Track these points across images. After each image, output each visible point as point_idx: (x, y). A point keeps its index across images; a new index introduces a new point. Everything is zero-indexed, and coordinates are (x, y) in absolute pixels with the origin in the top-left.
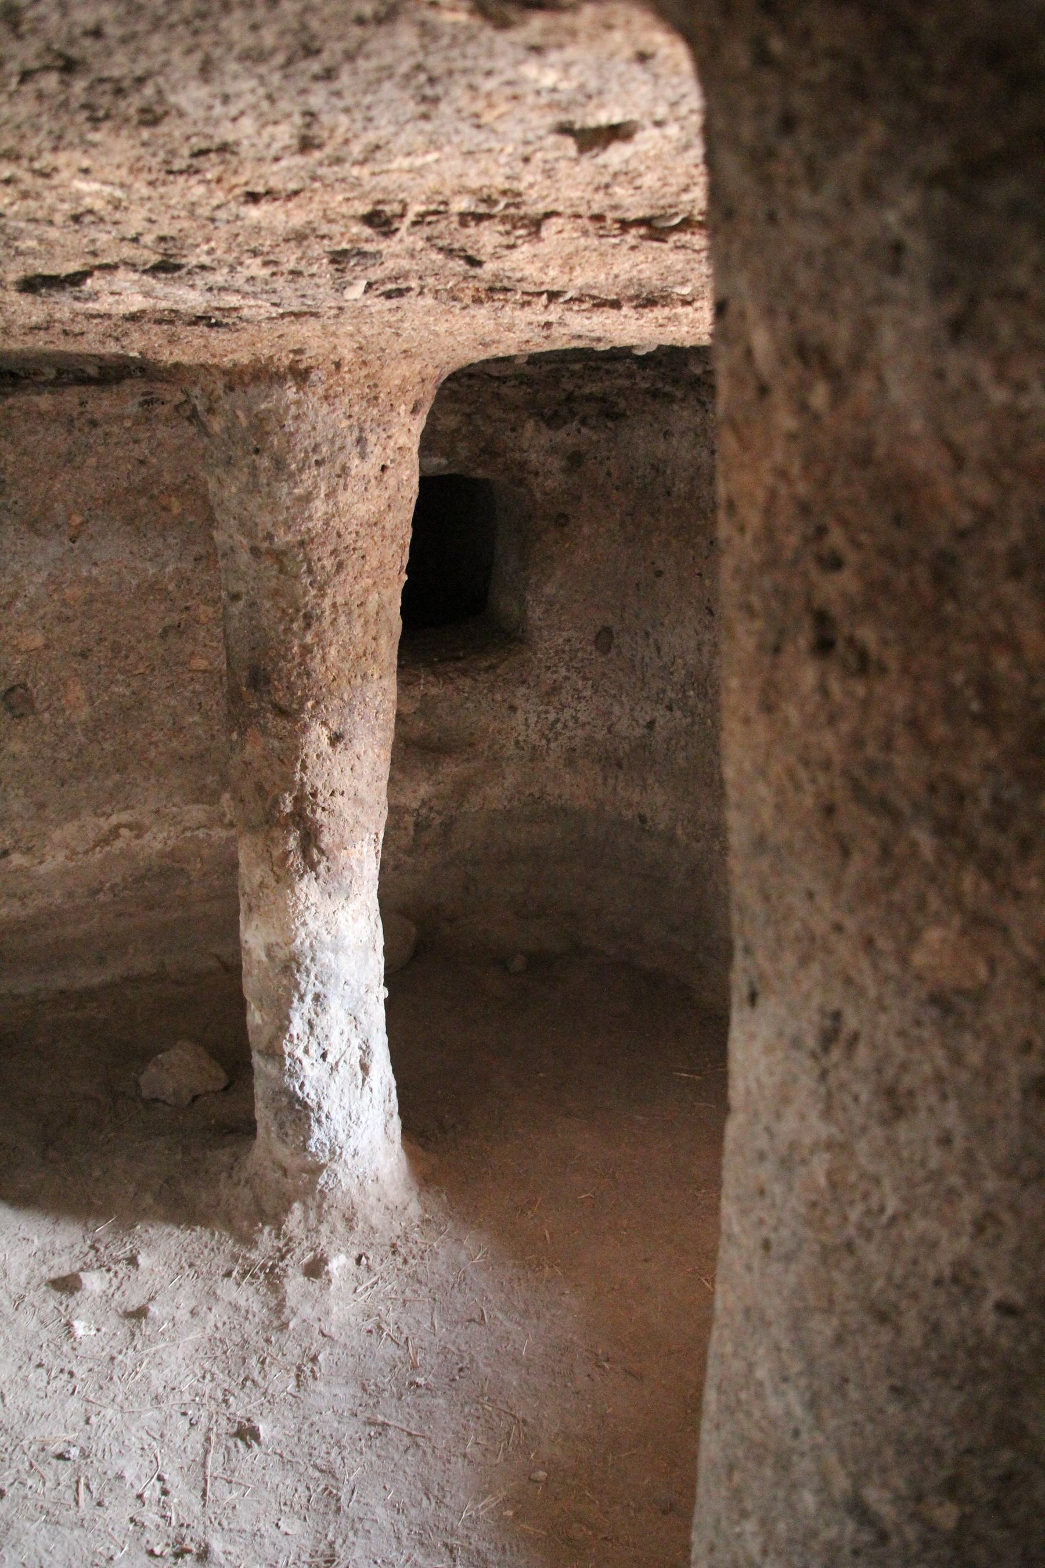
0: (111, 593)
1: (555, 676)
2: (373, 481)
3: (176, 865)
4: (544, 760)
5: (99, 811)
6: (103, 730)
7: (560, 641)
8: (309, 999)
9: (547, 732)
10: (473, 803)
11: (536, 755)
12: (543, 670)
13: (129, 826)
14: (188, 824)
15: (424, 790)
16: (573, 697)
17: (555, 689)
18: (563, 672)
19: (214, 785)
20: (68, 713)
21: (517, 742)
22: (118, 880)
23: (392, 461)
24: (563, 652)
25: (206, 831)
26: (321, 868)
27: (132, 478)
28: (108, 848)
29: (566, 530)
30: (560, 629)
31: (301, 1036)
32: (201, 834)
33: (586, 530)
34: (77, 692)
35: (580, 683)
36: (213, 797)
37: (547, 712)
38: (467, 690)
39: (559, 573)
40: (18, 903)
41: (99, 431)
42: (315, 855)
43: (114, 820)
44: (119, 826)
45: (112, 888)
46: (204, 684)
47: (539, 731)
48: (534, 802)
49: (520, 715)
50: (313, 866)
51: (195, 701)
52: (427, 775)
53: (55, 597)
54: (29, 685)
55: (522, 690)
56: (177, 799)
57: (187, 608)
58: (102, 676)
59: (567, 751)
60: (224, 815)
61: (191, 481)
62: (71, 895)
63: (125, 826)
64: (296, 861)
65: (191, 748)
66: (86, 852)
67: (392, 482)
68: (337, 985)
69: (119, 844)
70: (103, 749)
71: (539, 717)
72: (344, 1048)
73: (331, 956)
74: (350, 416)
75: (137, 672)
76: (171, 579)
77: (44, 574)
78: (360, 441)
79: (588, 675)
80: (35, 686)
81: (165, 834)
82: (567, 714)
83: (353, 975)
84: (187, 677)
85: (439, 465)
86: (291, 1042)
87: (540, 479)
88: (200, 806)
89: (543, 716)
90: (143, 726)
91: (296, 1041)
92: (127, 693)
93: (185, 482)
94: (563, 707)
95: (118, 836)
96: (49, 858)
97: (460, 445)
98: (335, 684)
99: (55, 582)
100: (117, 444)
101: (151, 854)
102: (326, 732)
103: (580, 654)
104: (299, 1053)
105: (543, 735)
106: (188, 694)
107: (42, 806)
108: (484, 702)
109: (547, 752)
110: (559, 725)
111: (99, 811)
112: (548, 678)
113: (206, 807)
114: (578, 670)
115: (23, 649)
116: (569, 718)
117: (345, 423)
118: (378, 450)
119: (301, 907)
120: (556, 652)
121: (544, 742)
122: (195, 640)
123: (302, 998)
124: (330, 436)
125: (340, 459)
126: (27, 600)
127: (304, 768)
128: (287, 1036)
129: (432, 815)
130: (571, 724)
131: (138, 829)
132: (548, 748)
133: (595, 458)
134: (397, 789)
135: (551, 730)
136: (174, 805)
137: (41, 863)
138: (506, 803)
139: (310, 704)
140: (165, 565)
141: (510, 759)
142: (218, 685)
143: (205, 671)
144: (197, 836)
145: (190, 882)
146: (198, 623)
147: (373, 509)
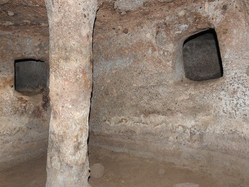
0: (119, 71)
1: (234, 87)
2: (57, 12)
4: (235, 118)
7: (233, 74)
9: (234, 108)
10: (210, 129)
11: (231, 116)
12: (229, 85)
14: (135, 121)
15: (193, 123)
16: (242, 94)
17: (235, 92)
18: (236, 85)
19: (139, 113)
21: (224, 111)
23: (61, 5)
24: (235, 78)
28: (121, 123)
29: (228, 34)
30: (232, 70)
33: (235, 32)
34: (115, 91)
35: (244, 89)
36: (139, 116)
37: (233, 100)
38: (203, 92)
39: (228, 50)
41: (112, 39)
43: (122, 117)
44: (122, 119)
45: (122, 132)
47: (231, 107)
48: (233, 134)
49: (223, 102)
51: (134, 93)
52: (193, 118)
53: (111, 72)
55: (223, 93)
56: (132, 115)
59: (243, 115)
62: (115, 131)
63: (124, 119)
65: (134, 104)
66: (117, 123)
67: (63, 11)
69: (123, 123)
71: (230, 102)
76: (128, 67)
77: (109, 68)
79: (246, 86)
82: (241, 101)
83: (57, 143)
84: (132, 88)
85: (186, 27)
87: (214, 20)
89: (232, 102)
92: (122, 91)
94: (239, 98)
97: (189, 19)
99: (111, 69)
103: (242, 78)
105: (233, 109)
106: (133, 92)
108: (210, 96)
109: (236, 115)
110: (238, 105)
112: (231, 88)
114: (242, 84)
116: (242, 102)
118: (56, 4)
120: (232, 78)
121: (234, 111)
129: (196, 131)
130: (243, 105)
132: (236, 114)
133: (230, 4)
134: (184, 121)
135: (235, 107)
138: (222, 132)
140: (127, 64)
141: (222, 116)
145: (136, 135)
147: (59, 19)
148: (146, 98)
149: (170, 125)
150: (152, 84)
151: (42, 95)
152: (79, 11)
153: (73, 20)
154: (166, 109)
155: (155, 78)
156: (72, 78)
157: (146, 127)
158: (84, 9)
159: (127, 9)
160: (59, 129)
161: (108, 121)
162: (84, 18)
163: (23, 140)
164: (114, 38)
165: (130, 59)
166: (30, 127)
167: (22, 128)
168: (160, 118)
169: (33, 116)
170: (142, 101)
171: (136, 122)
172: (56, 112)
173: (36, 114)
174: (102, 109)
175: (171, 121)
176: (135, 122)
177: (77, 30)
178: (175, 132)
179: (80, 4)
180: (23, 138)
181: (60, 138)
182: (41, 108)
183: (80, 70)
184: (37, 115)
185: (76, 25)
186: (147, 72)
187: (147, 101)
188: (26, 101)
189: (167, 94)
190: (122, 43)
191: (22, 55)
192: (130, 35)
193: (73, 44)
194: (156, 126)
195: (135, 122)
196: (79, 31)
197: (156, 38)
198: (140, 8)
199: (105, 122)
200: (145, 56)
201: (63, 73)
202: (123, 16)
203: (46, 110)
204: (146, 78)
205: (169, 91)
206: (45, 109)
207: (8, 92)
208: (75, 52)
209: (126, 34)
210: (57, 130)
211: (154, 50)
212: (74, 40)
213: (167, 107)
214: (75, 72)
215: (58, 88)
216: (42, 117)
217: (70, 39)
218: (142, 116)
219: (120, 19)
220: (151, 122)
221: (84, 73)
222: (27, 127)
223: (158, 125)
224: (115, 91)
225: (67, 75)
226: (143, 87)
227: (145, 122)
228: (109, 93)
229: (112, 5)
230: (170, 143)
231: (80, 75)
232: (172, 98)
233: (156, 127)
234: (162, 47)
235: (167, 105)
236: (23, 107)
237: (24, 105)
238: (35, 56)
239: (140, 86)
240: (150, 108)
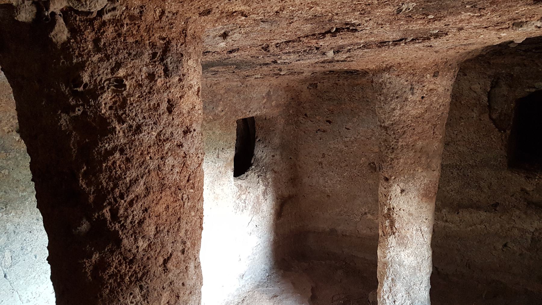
2: (418, 102)
8: (390, 279)
23: (426, 95)
26: (396, 234)
31: (387, 291)
40: (369, 230)
42: (395, 230)
50: (394, 233)
60: (443, 217)
64: (388, 230)
68: (400, 278)
72: (403, 302)
73: (398, 267)
74: (407, 81)
78: (412, 89)
83: (407, 277)
86: (384, 292)
91: (385, 293)
98: (402, 172)
102: (399, 188)
104: (386, 297)
117: (406, 83)
119: (389, 246)
123: (387, 278)
124: (401, 88)
125: (405, 95)
127: (391, 199)
128: (382, 290)
137: (377, 219)
139: (393, 178)
150: (471, 162)
151: (256, 175)
168: (483, 215)
174: (359, 194)
182: (261, 197)
199: (365, 216)
203: (266, 200)
207: (229, 180)
210: (407, 261)
220: (461, 220)
227: (448, 220)
233: (469, 229)
234: (496, 108)
236: (243, 201)
237: (243, 197)
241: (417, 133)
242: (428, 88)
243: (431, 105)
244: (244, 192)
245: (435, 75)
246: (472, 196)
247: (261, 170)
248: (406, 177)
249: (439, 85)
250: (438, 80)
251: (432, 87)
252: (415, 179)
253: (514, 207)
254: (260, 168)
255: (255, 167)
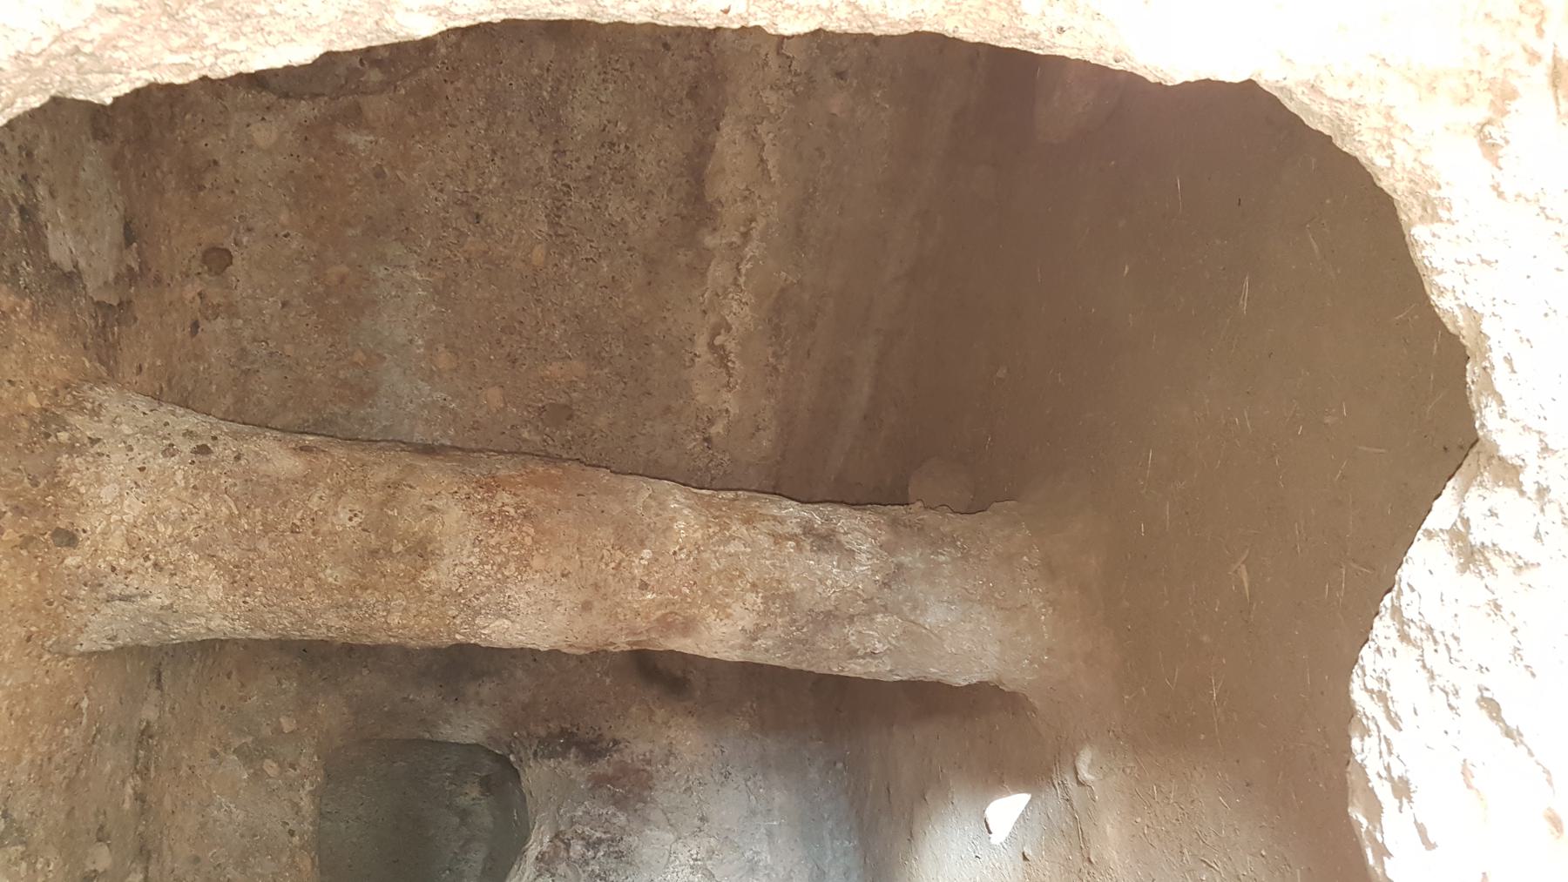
2: (177, 579)
3: (774, 295)
5: (687, 364)
6: (599, 353)
13: (715, 333)
14: (731, 280)
20: (574, 379)
22: (770, 350)
23: (147, 558)
25: (745, 262)
27: (304, 313)
32: (744, 268)
34: (554, 369)
36: (705, 256)
40: (762, 432)
43: (701, 347)
44: (711, 346)
45: (775, 354)
46: (562, 256)
54: (540, 405)
56: (697, 293)
57: (468, 261)
58: (539, 347)
61: (304, 256)
62: (770, 391)
63: (713, 337)
66: (730, 376)
67: (175, 552)
69: (731, 346)
70: (620, 355)
75: (540, 315)
76: (430, 275)
80: (542, 401)
81: (734, 304)
88: (712, 268)
90: (603, 316)
93: (307, 262)
95: (722, 347)
96: (726, 405)
100: (264, 329)
101: (752, 317)
106: (574, 269)
107: (668, 409)
111: (687, 364)
113: (713, 263)
115: (502, 405)
118: (134, 581)
122: (507, 258)
126: (450, 398)
131: (722, 327)
136: (703, 296)
137: (727, 411)
140: (414, 280)
142: (567, 240)
143: (548, 253)
144: (745, 282)
145: (800, 283)
146: (487, 253)
147: (213, 575)
148: (617, 206)
149: (771, 97)
150: (544, 158)
152: (179, 476)
153: (229, 508)
154: (688, 105)
155: (513, 135)
156: (516, 534)
157: (768, 226)
158: (169, 451)
159: (119, 237)
160: (738, 609)
161: (711, 422)
162: (213, 457)
163: (757, 853)
164: (247, 333)
165: (382, 259)
166: (697, 822)
167: (696, 860)
169: (640, 805)
170: (632, 227)
171: (736, 279)
172: (664, 616)
173: (630, 791)
175: (754, 88)
176: (735, 283)
177: (277, 491)
178: (811, 80)
179: (142, 469)
180: (748, 854)
181: (776, 607)
182: (603, 767)
183: (482, 500)
184: (636, 790)
185: (255, 497)
186: (472, 176)
187: (635, 203)
188: (557, 836)
189: (611, 87)
190: (282, 291)
191: (302, 847)
192: (245, 240)
193: (350, 519)
194: (766, 172)
195: (735, 283)
196: (282, 487)
197: (287, 96)
198: (116, 162)
199: (715, 440)
200: (379, 174)
201: (488, 576)
202: (144, 265)
203: (616, 742)
204: (507, 186)
205: (594, 74)
206: (608, 750)
208: (390, 513)
209: (237, 261)
210: (742, 619)
211: (355, 118)
212: (331, 513)
213: (681, 102)
214: (492, 520)
215: (557, 603)
216: (649, 762)
217: (325, 528)
218: (710, 241)
219: (158, 280)
221: (491, 485)
222: (694, 834)
223: (762, 160)
224: (554, 369)
225: (499, 559)
226: (558, 209)
227: (742, 229)
228: (563, 400)
229: (105, 316)
230: (859, 114)
231: (506, 501)
232: (632, 65)
233: (775, 176)
235: (666, 95)
236: (591, 854)
237: (578, 848)
238: (308, 787)
239: (545, 228)
240: (670, 190)
241: (292, 584)
242: (122, 555)
243: (188, 541)
244: (563, 846)
245: (69, 539)
246: (662, 163)
247: (521, 743)
248: (453, 612)
249: (114, 517)
250: (93, 523)
251: (117, 542)
252: (461, 590)
253: (708, 44)
254: (517, 741)
255: (512, 752)
